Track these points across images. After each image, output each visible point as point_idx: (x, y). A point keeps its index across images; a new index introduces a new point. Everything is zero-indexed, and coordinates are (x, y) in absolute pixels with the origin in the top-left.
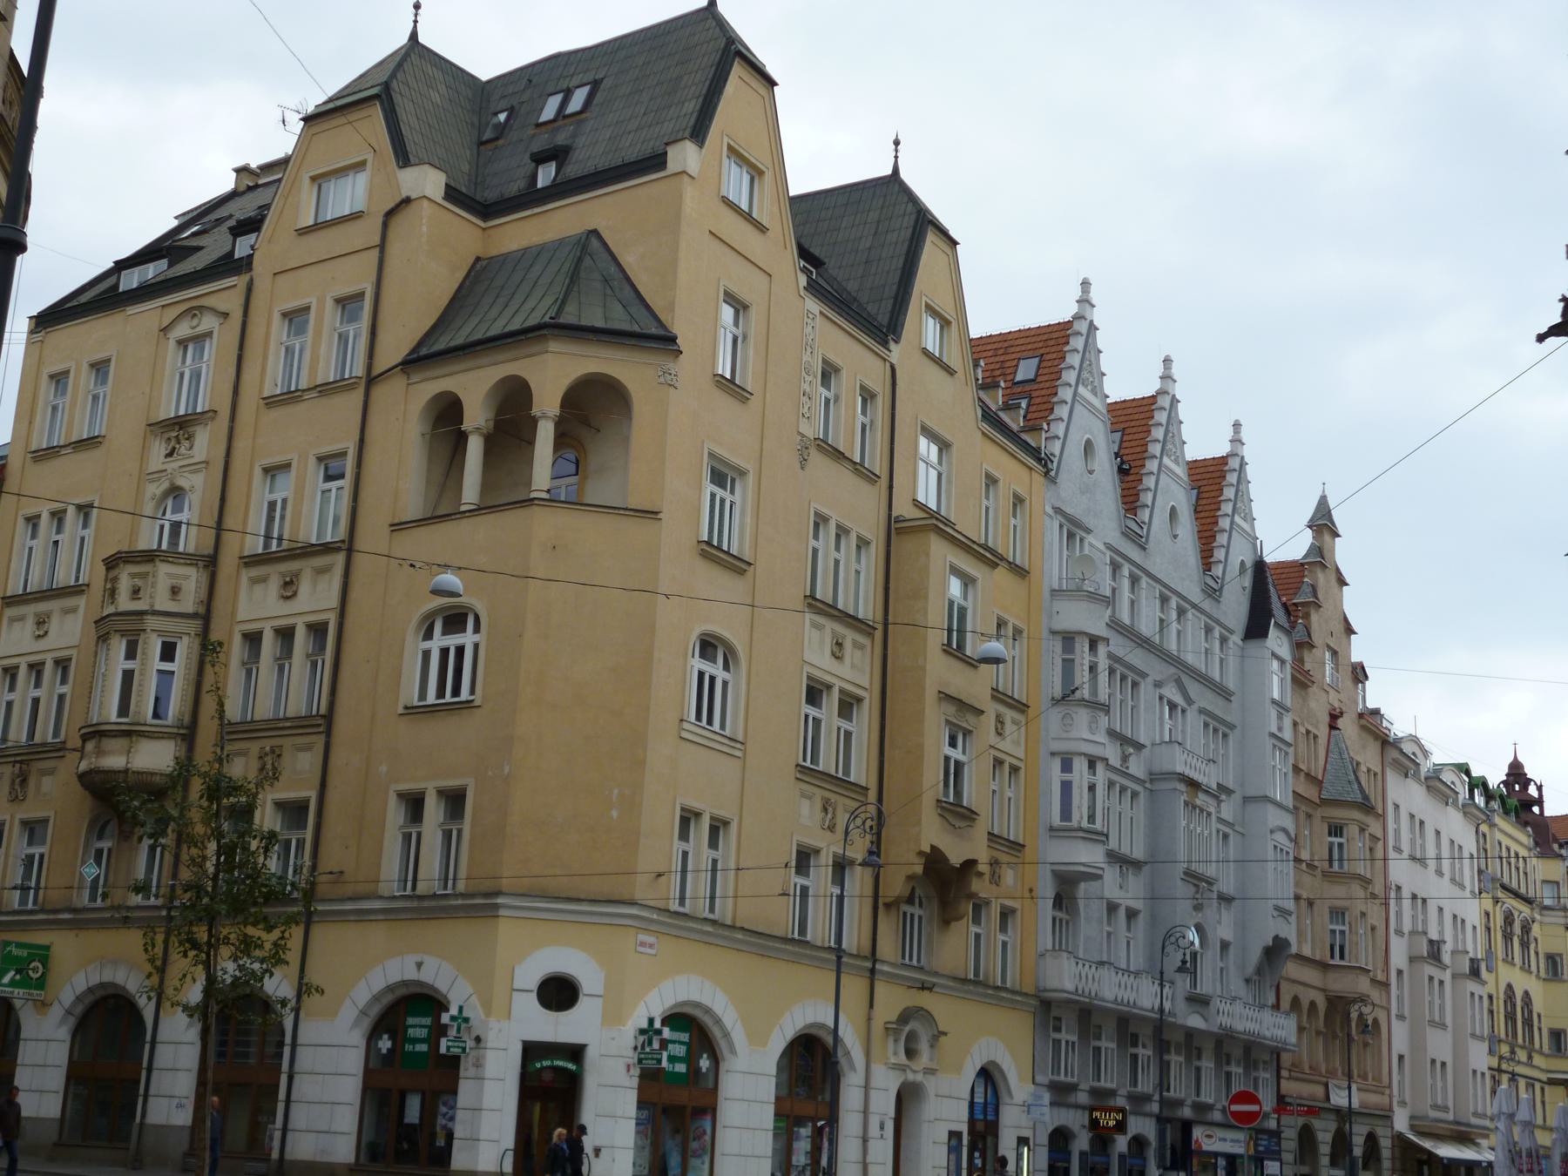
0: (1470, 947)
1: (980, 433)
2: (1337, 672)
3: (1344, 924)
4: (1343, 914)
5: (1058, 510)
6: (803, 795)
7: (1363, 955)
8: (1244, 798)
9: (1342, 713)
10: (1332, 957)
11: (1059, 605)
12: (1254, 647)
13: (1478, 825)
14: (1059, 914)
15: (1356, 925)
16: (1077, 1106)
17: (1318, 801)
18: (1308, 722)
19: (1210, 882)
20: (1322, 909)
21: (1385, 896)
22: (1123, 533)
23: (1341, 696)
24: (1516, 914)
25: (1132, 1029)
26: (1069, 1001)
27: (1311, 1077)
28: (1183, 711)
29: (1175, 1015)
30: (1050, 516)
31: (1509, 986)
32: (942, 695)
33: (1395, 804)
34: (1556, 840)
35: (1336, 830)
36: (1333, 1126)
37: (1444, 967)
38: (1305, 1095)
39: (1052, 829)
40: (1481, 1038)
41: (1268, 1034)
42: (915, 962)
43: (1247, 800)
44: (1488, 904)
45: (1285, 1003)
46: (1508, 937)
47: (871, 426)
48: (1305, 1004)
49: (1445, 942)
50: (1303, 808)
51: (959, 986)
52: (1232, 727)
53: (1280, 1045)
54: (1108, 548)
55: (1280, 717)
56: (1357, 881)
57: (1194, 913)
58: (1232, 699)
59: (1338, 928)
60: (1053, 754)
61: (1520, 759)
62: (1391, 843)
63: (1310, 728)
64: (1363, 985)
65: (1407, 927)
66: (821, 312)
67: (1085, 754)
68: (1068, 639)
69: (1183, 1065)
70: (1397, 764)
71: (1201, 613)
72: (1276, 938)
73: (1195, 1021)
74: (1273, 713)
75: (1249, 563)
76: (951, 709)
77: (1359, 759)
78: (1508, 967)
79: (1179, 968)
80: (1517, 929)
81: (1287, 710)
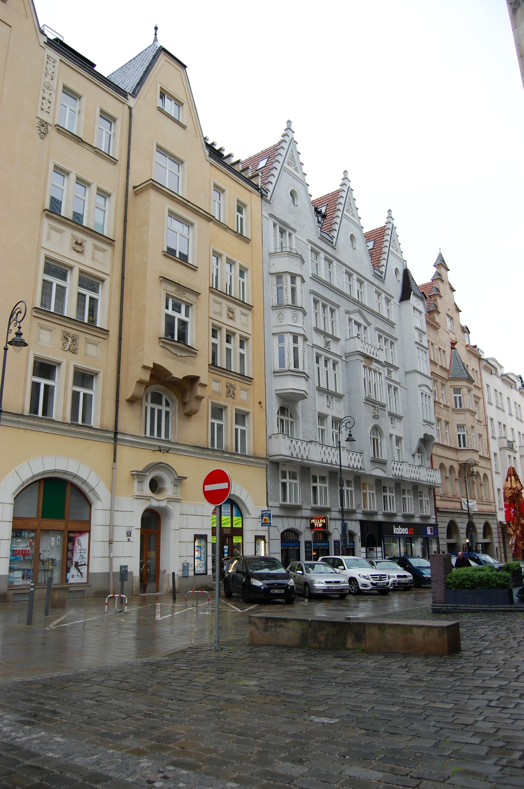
2: (453, 326)
3: (464, 431)
4: (464, 427)
5: (271, 216)
6: (42, 327)
7: (473, 442)
9: (456, 342)
10: (460, 446)
11: (273, 261)
12: (405, 304)
14: (285, 418)
15: (470, 431)
16: (302, 518)
17: (448, 379)
19: (383, 406)
20: (453, 426)
21: (485, 422)
22: (319, 238)
25: (383, 484)
27: (453, 499)
28: (365, 328)
29: (364, 470)
30: (267, 218)
32: (161, 279)
33: (487, 385)
35: (457, 390)
36: (467, 521)
37: (516, 452)
38: (450, 507)
39: (274, 372)
41: (425, 479)
42: (163, 437)
43: (406, 373)
45: (436, 465)
47: (114, 135)
48: (447, 467)
50: (440, 381)
52: (396, 339)
53: (432, 484)
54: (309, 242)
55: (420, 336)
56: (468, 412)
57: (374, 420)
58: (395, 326)
59: (461, 433)
60: (273, 334)
62: (486, 400)
63: (441, 347)
64: (475, 457)
65: (497, 435)
66: (60, 60)
67: (290, 333)
68: (279, 276)
69: (394, 497)
70: (485, 368)
71: (373, 285)
72: (425, 435)
73: (378, 473)
74: (416, 333)
75: (401, 272)
76: (171, 289)
79: (348, 439)
81: (425, 333)
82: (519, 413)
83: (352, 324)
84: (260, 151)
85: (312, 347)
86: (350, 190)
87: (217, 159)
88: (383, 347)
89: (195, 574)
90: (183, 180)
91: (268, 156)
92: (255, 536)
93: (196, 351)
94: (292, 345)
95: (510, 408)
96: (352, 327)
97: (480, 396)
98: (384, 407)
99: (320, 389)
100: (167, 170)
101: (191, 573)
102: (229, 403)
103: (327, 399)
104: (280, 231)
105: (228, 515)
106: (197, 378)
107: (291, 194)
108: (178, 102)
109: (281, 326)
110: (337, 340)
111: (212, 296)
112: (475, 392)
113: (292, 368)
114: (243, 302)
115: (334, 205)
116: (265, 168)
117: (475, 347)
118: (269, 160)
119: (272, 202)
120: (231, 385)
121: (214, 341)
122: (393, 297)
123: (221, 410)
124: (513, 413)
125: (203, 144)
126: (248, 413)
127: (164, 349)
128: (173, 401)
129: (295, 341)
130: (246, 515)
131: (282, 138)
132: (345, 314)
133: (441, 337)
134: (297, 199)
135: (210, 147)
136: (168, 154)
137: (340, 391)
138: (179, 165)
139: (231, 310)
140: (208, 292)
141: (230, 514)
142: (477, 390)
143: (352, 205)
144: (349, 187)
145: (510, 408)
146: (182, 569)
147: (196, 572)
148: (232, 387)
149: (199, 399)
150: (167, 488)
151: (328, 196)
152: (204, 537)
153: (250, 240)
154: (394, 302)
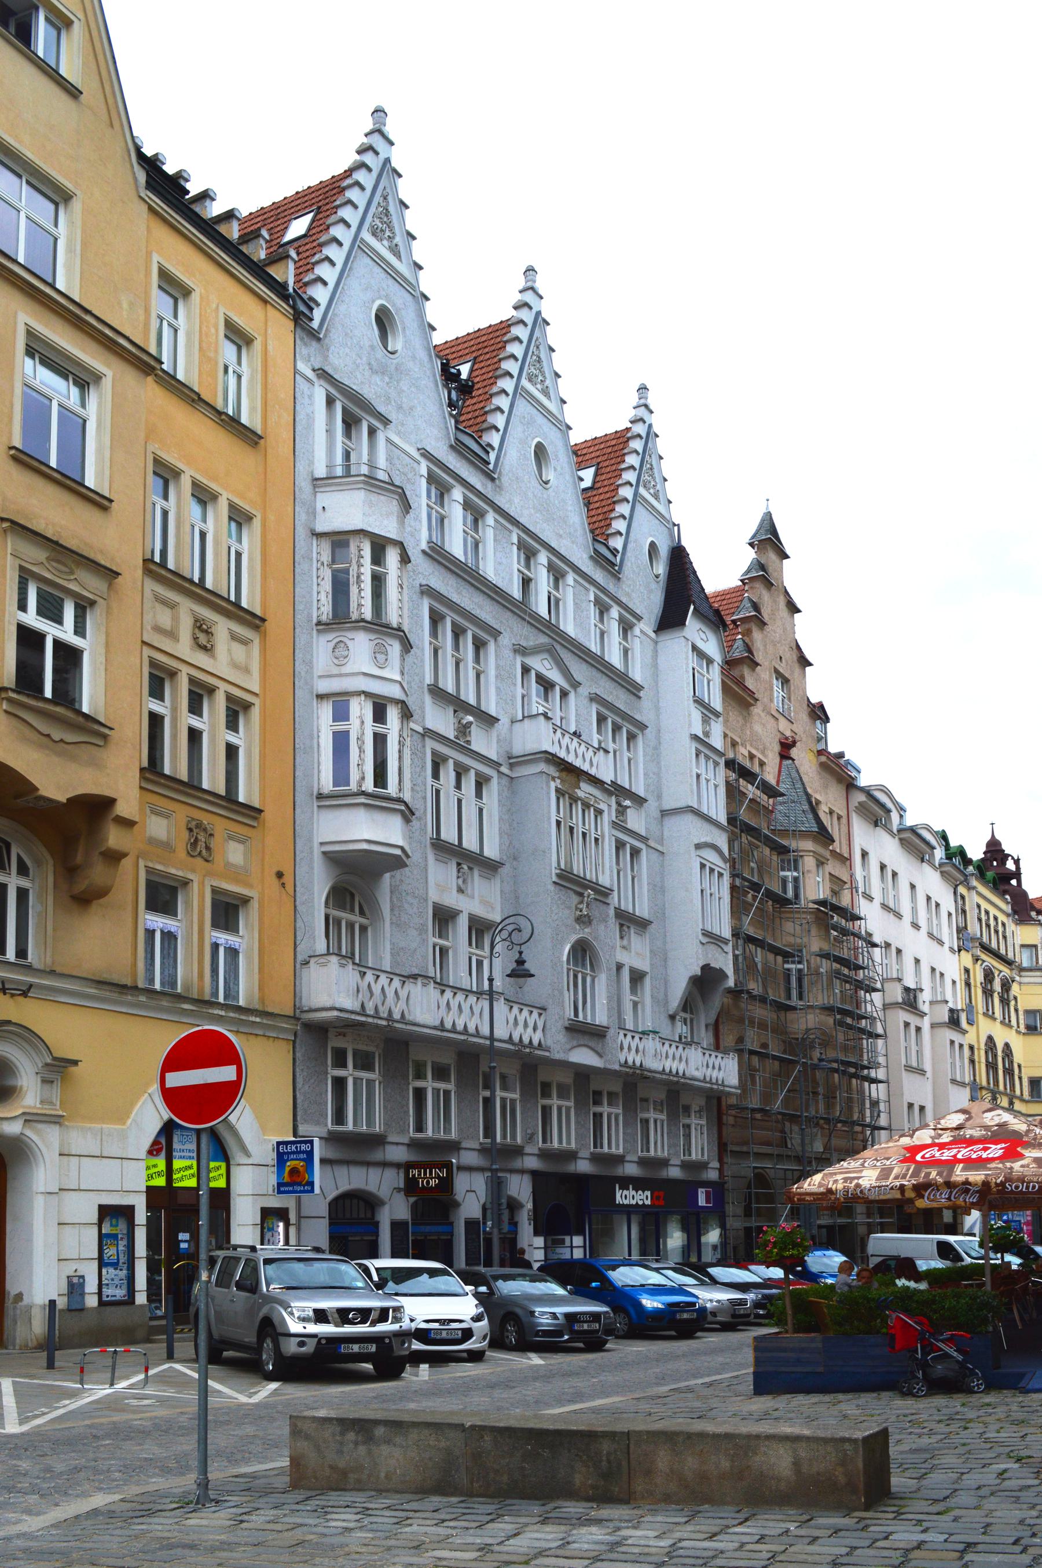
0: (949, 996)
1: (145, 208)
2: (789, 699)
8: (662, 811)
13: (957, 886)
18: (751, 745)
23: (794, 727)
24: (996, 973)
26: (700, 1090)
28: (564, 694)
31: (990, 1039)
34: (1033, 908)
39: (320, 797)
40: (962, 1084)
43: (665, 813)
44: (967, 959)
46: (988, 993)
49: (921, 990)
51: (115, 996)
52: (642, 727)
55: (706, 720)
58: (642, 694)
61: (997, 837)
63: (754, 752)
67: (367, 694)
70: (862, 809)
74: (696, 715)
77: (819, 797)
78: (988, 1021)
80: (997, 986)
82: (935, 922)
83: (529, 681)
84: (290, 192)
85: (423, 736)
86: (540, 322)
87: (169, 197)
88: (554, 712)
89: (101, 1303)
90: (70, 250)
91: (314, 207)
92: (262, 1209)
93: (106, 731)
94: (370, 728)
95: (914, 910)
96: (529, 688)
97: (845, 877)
98: (606, 895)
99: (440, 846)
100: (23, 215)
101: (92, 1301)
102: (193, 871)
103: (459, 871)
104: (344, 421)
105: (190, 1158)
106: (110, 802)
107: (378, 318)
108: (57, 17)
109: (341, 675)
110: (490, 720)
111: (151, 586)
112: (833, 867)
113: (369, 785)
114: (237, 605)
115: (496, 360)
116: (307, 240)
117: (841, 755)
118: (318, 217)
119: (325, 336)
120: (199, 825)
121: (155, 706)
122: (639, 618)
123: (173, 891)
124: (922, 922)
125: (129, 151)
126: (246, 901)
127: (14, 722)
128: (39, 863)
129: (379, 716)
130: (238, 1157)
131: (357, 157)
132: (511, 654)
133: (758, 728)
134: (394, 334)
135: (152, 165)
136: (25, 170)
137: (491, 851)
138: (57, 204)
139: (204, 627)
140: (140, 572)
141: (195, 1155)
142: (838, 864)
143: (545, 364)
144: (539, 313)
145: (914, 910)
146: (66, 1292)
147: (105, 1299)
148: (205, 830)
149: (115, 857)
150: (25, 1089)
151: (478, 335)
152: (127, 1212)
153: (261, 437)
154: (642, 631)
